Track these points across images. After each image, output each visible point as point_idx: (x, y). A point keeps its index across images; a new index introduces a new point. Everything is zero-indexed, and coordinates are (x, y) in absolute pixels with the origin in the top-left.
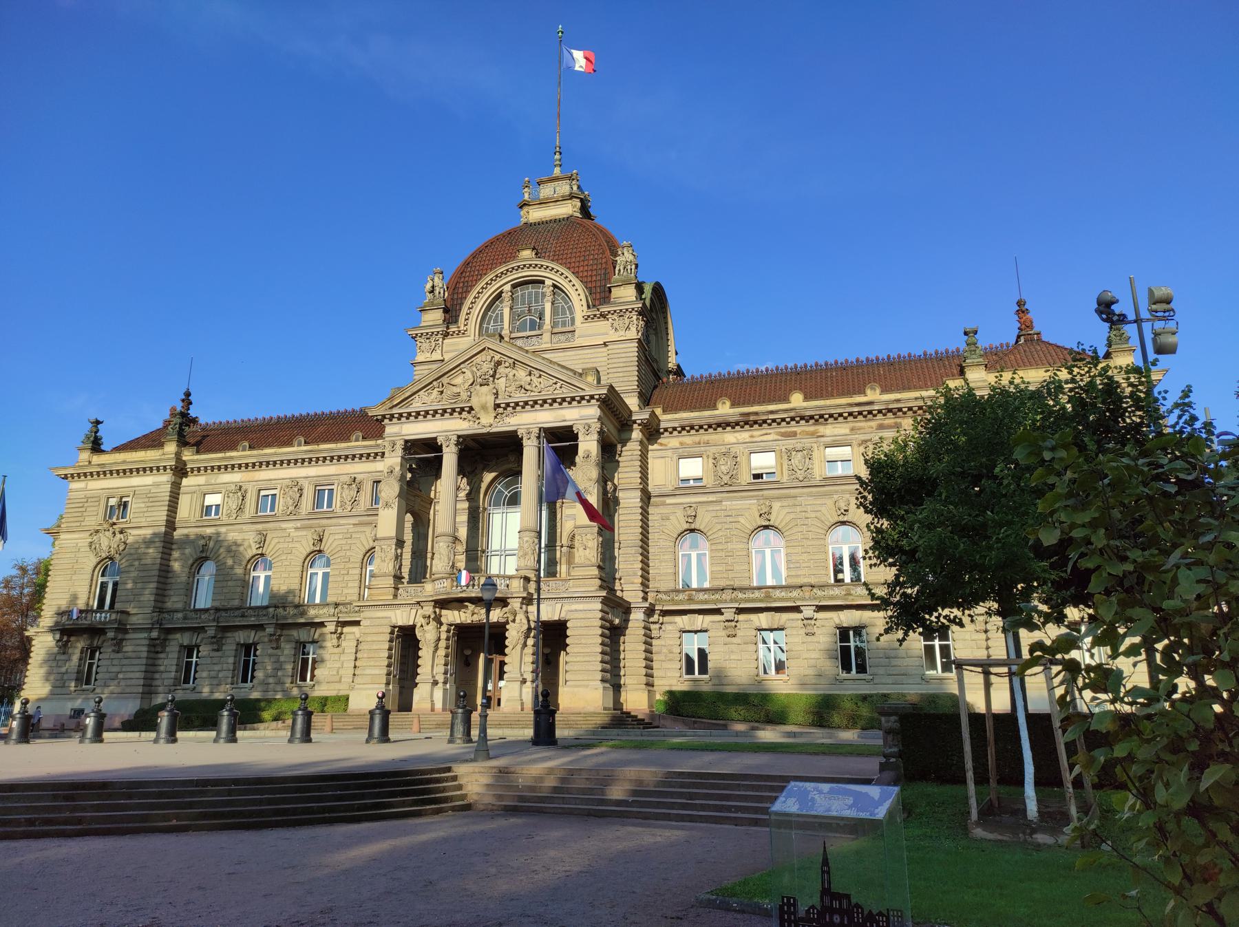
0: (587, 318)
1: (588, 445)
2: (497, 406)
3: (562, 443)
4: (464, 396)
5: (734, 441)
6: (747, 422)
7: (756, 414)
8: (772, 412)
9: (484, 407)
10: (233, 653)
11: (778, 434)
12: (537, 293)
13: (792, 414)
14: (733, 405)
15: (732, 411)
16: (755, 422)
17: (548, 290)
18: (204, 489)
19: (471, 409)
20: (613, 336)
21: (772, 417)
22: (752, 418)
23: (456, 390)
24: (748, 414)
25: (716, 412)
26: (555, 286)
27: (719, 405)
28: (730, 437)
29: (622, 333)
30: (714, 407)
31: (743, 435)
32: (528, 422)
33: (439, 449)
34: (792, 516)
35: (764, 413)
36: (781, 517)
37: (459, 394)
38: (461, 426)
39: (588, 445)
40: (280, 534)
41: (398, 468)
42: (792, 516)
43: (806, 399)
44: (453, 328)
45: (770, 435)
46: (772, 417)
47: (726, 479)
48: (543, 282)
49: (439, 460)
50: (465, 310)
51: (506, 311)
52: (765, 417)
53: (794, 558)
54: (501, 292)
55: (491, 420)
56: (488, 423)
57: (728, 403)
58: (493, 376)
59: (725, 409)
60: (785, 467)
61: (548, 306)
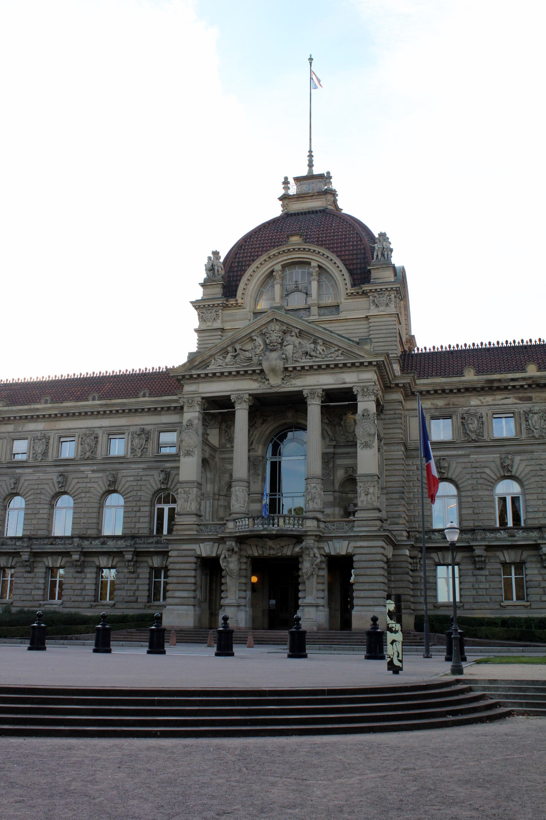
0: (351, 295)
2: (286, 369)
3: (339, 404)
4: (255, 360)
5: (479, 403)
6: (490, 388)
7: (499, 380)
8: (513, 380)
9: (273, 370)
10: (43, 575)
11: (516, 398)
12: (303, 273)
13: (530, 382)
14: (478, 373)
15: (476, 378)
16: (498, 388)
18: (13, 435)
19: (262, 371)
20: (374, 311)
21: (512, 384)
22: (496, 384)
23: (248, 354)
24: (492, 381)
25: (463, 379)
26: (319, 267)
27: (466, 373)
28: (474, 401)
29: (381, 308)
30: (462, 374)
31: (489, 399)
33: (232, 405)
34: (529, 468)
35: (506, 380)
36: (521, 469)
37: (250, 359)
38: (252, 386)
40: (79, 475)
41: (196, 422)
42: (529, 468)
44: (232, 302)
45: (510, 400)
46: (512, 384)
47: (474, 437)
48: (309, 264)
49: (232, 416)
51: (277, 288)
52: (506, 384)
53: (532, 503)
54: (273, 271)
55: (279, 382)
56: (276, 384)
57: (472, 372)
58: (281, 344)
60: (524, 426)
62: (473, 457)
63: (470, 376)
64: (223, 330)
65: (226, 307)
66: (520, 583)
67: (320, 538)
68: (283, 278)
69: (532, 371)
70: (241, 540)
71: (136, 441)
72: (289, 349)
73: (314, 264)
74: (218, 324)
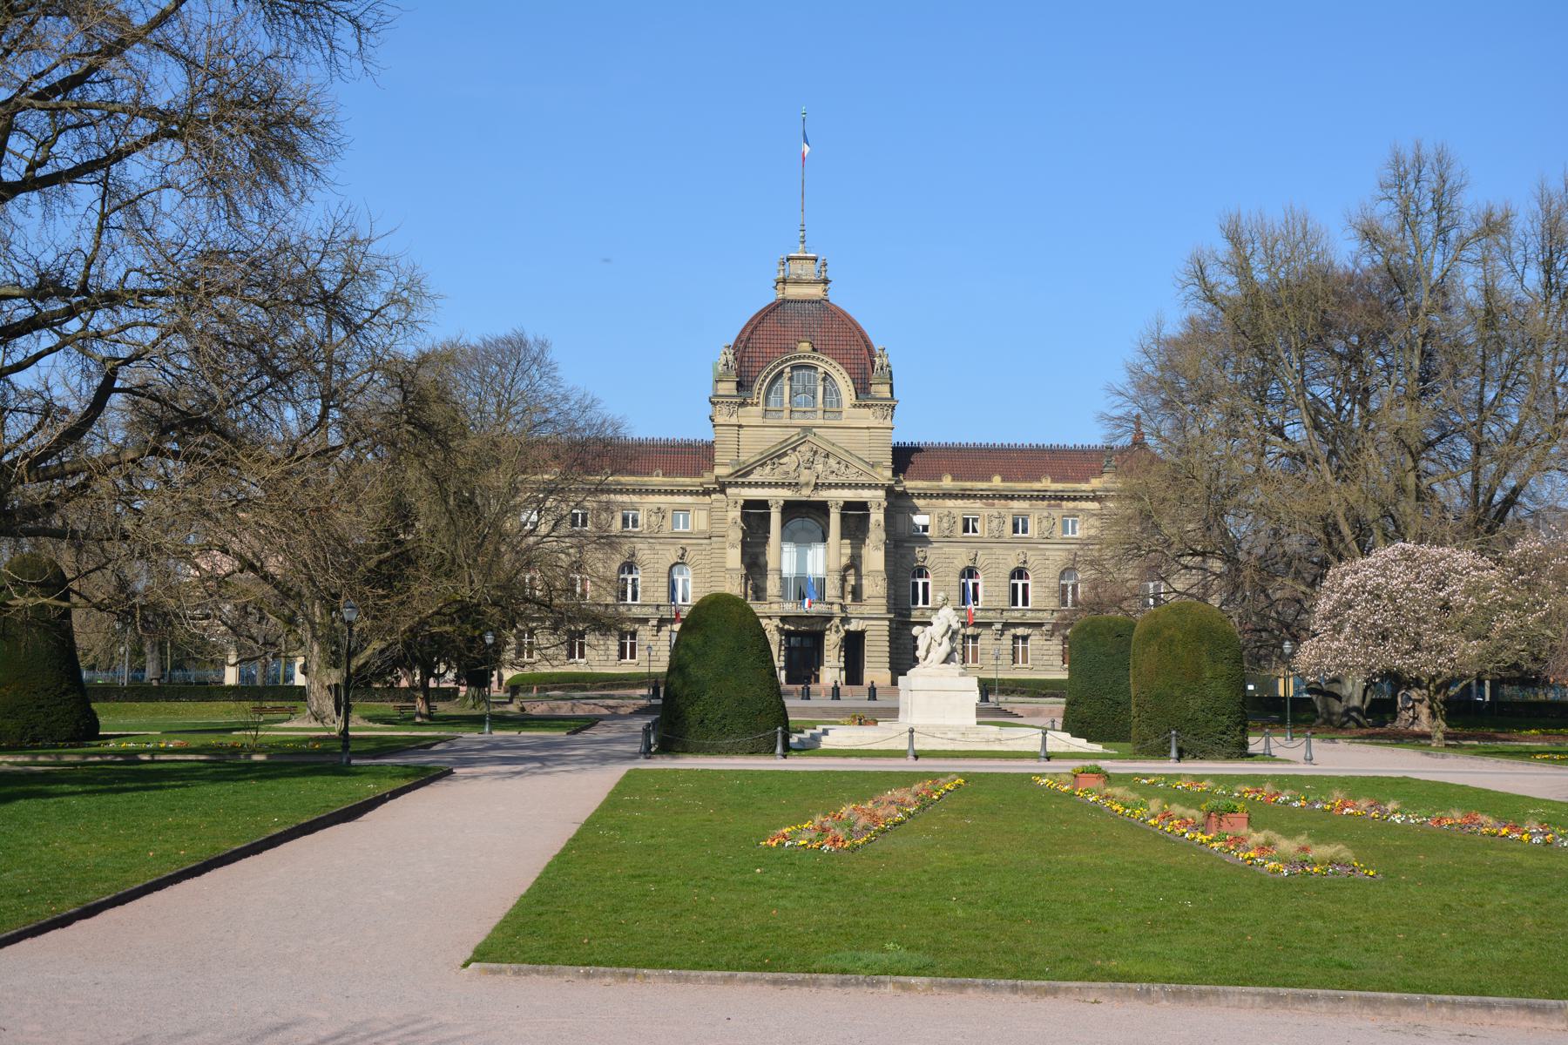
0: (855, 406)
1: (877, 517)
4: (792, 475)
9: (807, 484)
14: (953, 480)
17: (820, 377)
28: (950, 503)
31: (959, 502)
32: (836, 497)
38: (788, 494)
39: (877, 517)
43: (1003, 480)
50: (756, 386)
51: (787, 389)
56: (805, 494)
59: (947, 483)
61: (820, 390)
62: (946, 550)
63: (947, 483)
64: (740, 426)
65: (743, 404)
66: (975, 649)
67: (845, 620)
68: (791, 379)
69: (997, 482)
70: (784, 619)
71: (653, 518)
72: (820, 468)
73: (820, 370)
74: (734, 420)
